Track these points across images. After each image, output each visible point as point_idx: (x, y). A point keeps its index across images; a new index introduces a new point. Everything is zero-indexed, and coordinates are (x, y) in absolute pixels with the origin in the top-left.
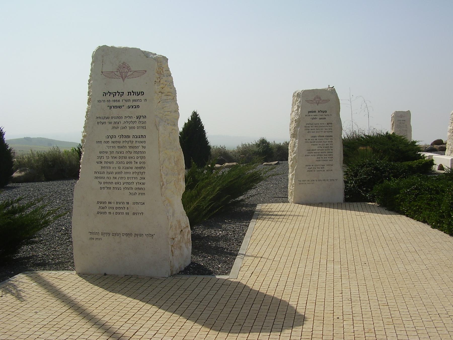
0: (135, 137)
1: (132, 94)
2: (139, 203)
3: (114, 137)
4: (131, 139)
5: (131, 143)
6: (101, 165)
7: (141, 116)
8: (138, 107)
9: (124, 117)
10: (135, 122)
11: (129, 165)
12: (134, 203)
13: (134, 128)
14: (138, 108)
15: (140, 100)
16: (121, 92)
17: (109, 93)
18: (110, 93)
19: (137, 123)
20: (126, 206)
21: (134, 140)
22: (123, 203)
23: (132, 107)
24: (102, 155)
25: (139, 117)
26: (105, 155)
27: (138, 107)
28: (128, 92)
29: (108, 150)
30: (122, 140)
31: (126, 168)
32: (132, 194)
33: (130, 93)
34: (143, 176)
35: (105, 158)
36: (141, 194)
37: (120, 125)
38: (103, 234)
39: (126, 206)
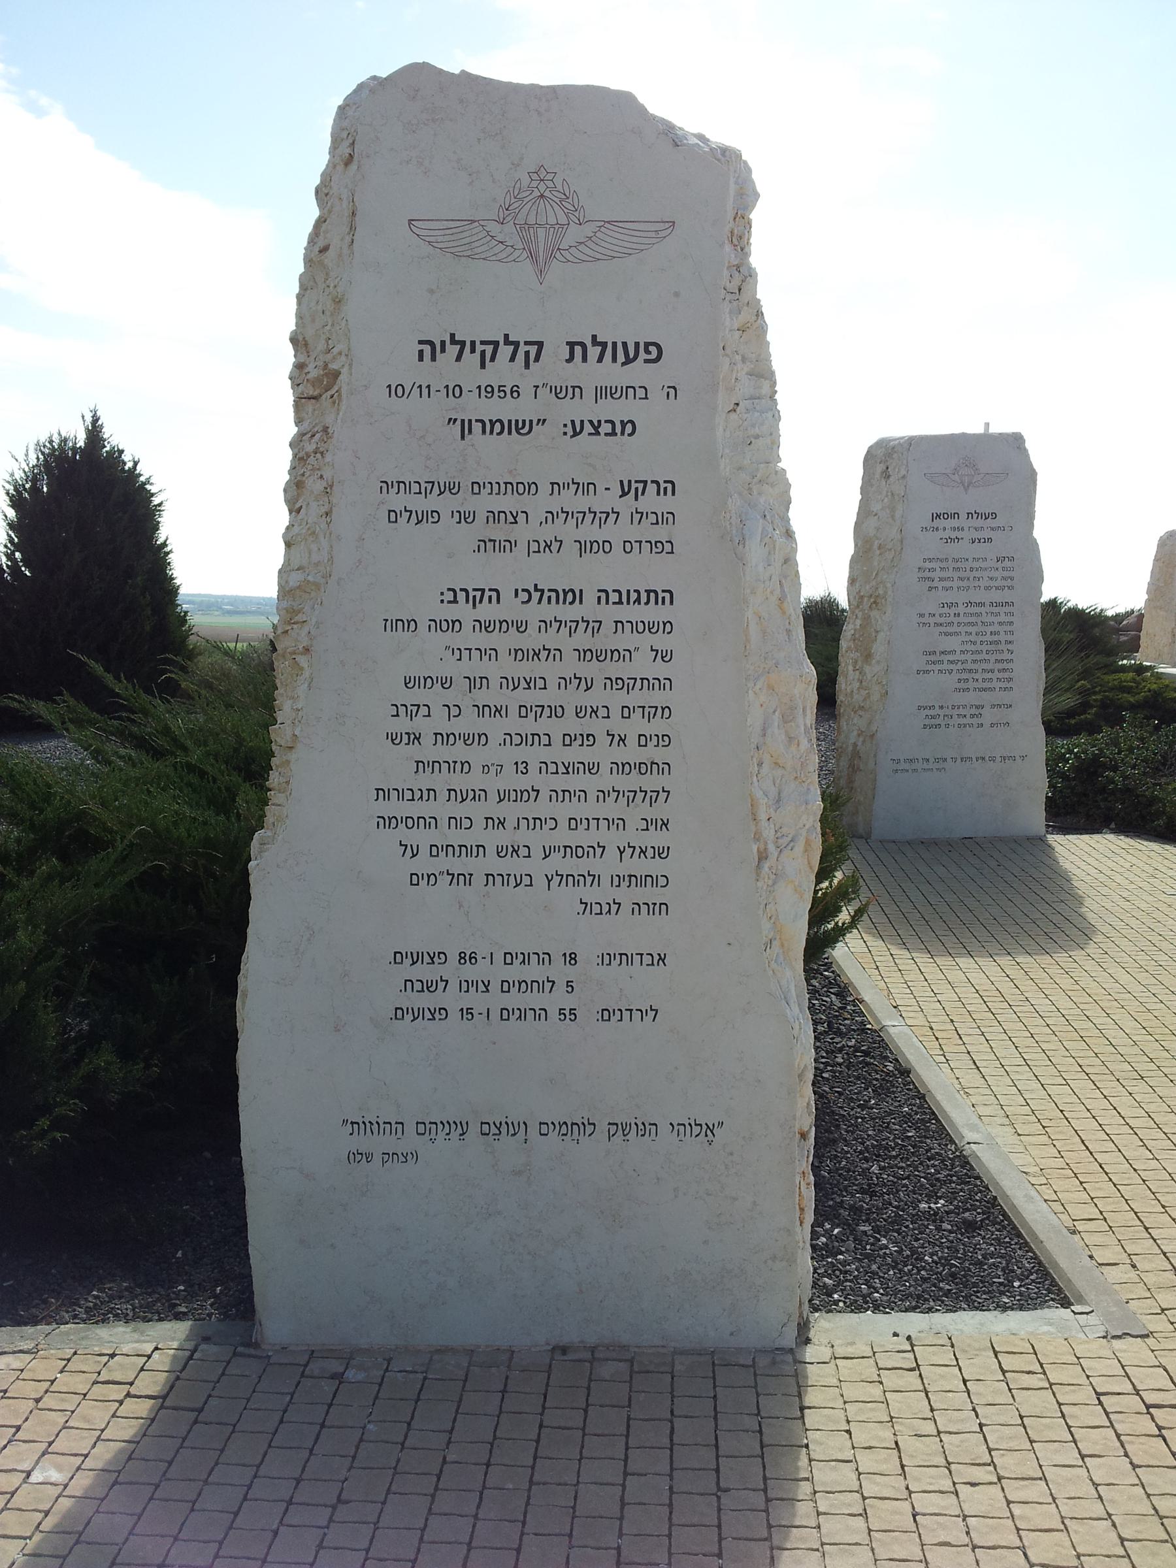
0: (614, 597)
1: (594, 352)
2: (637, 958)
4: (588, 609)
5: (590, 630)
6: (414, 751)
7: (645, 482)
9: (545, 488)
10: (613, 517)
11: (575, 754)
12: (607, 959)
13: (605, 546)
14: (630, 435)
15: (641, 393)
16: (526, 343)
17: (453, 341)
18: (463, 344)
19: (625, 517)
20: (559, 971)
21: (609, 613)
22: (545, 958)
24: (418, 695)
25: (634, 485)
26: (434, 697)
28: (568, 343)
29: (451, 668)
30: (536, 612)
31: (562, 769)
32: (596, 909)
33: (578, 350)
34: (659, 811)
35: (439, 712)
36: (644, 908)
37: (522, 533)
38: (425, 1128)
39: (559, 971)
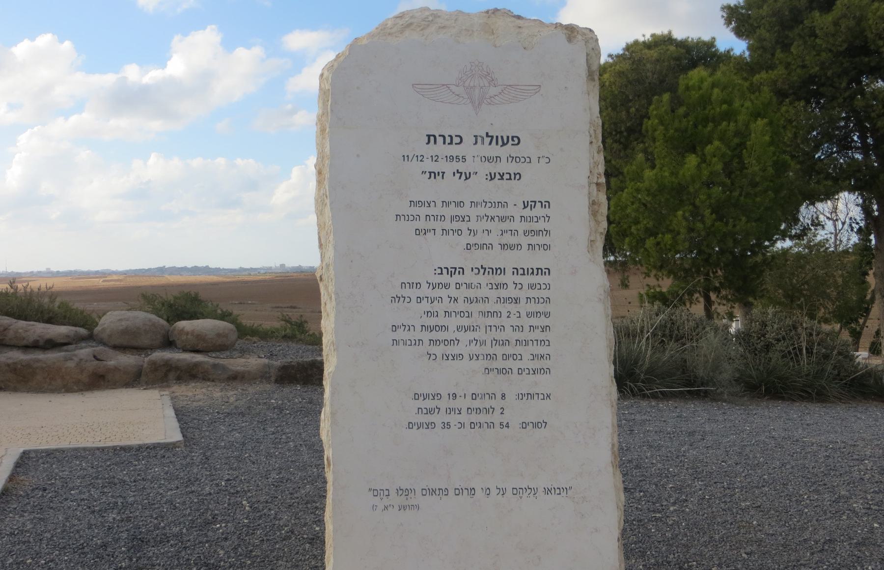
3: (459, 272)
8: (518, 177)
23: (500, 178)
25: (530, 203)
27: (518, 177)
30: (483, 279)
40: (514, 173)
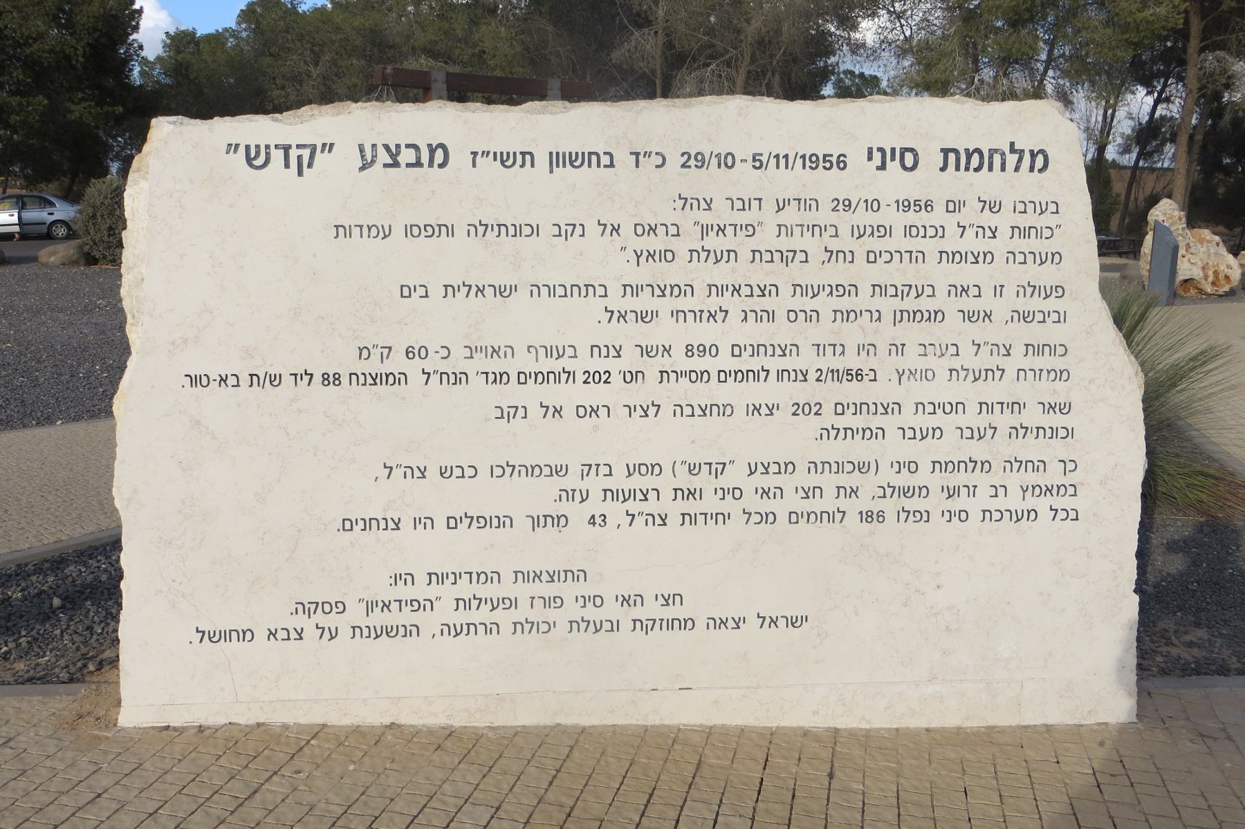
40: (430, 146)
